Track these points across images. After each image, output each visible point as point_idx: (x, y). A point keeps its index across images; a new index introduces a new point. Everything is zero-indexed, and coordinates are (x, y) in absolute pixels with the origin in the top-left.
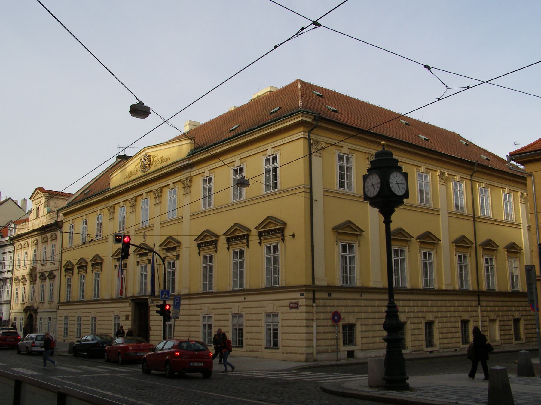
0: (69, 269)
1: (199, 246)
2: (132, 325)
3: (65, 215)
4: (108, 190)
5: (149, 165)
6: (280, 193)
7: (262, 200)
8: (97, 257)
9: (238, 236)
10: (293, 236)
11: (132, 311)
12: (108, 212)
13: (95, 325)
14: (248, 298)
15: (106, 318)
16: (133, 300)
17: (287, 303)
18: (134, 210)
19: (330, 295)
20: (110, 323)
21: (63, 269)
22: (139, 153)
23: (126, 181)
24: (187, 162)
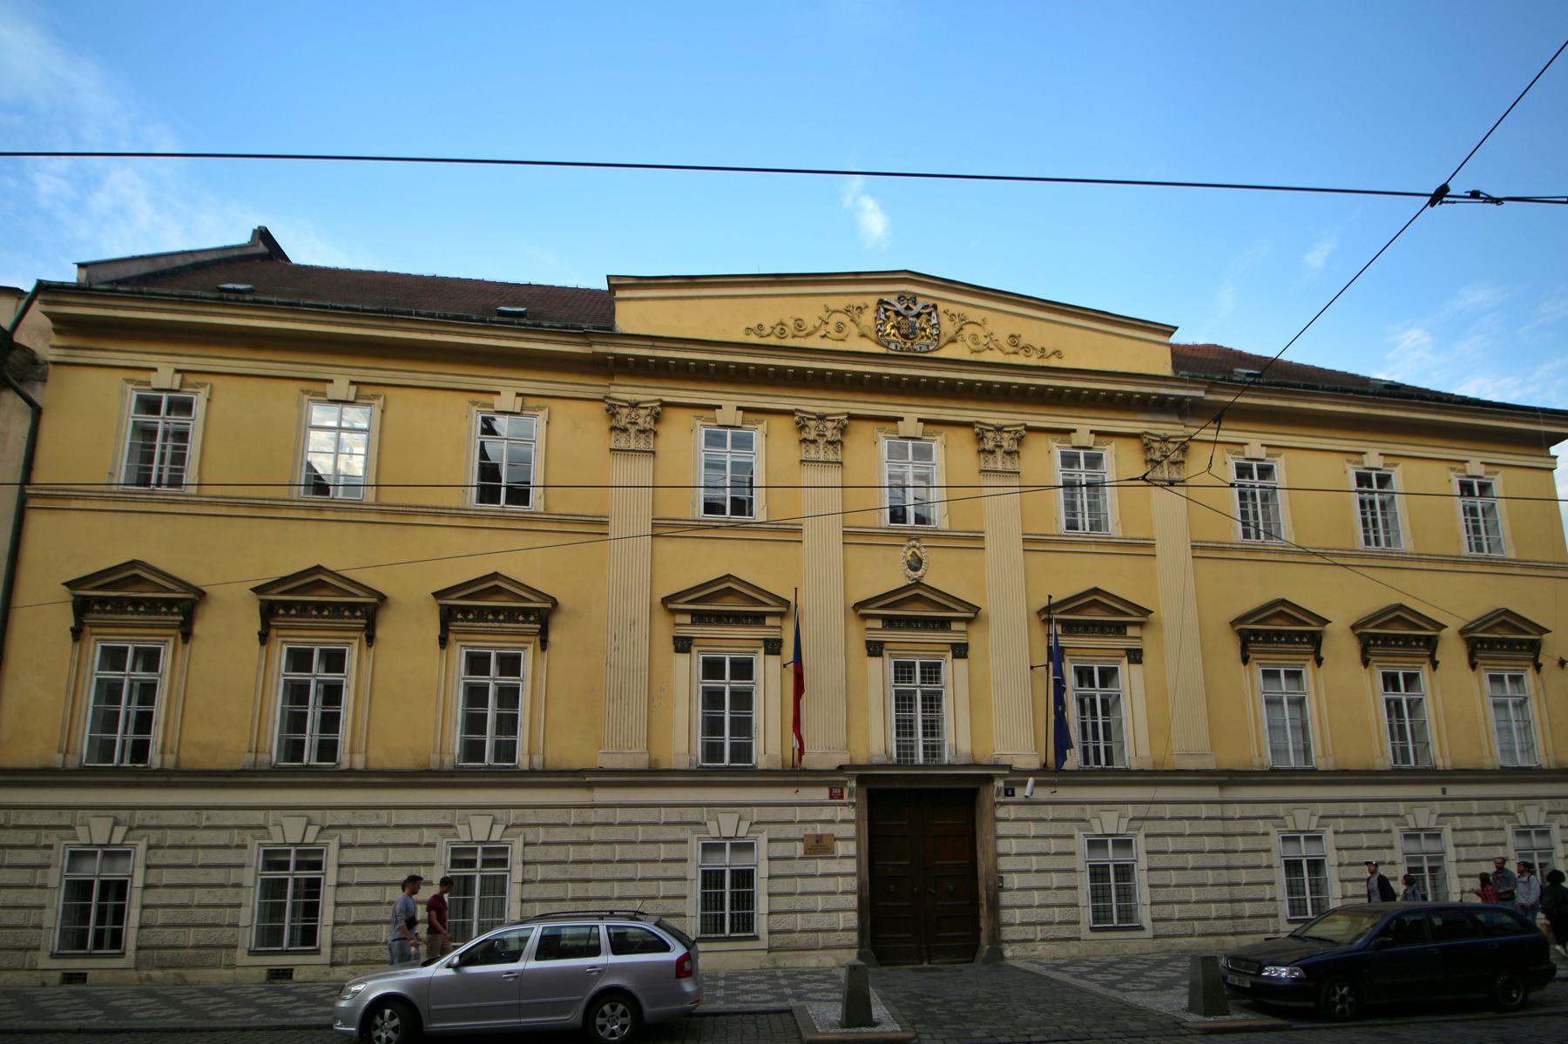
3: (65, 325)
4: (607, 330)
7: (1461, 568)
9: (1396, 638)
14: (1453, 791)
16: (861, 780)
19: (1444, 792)
23: (753, 339)
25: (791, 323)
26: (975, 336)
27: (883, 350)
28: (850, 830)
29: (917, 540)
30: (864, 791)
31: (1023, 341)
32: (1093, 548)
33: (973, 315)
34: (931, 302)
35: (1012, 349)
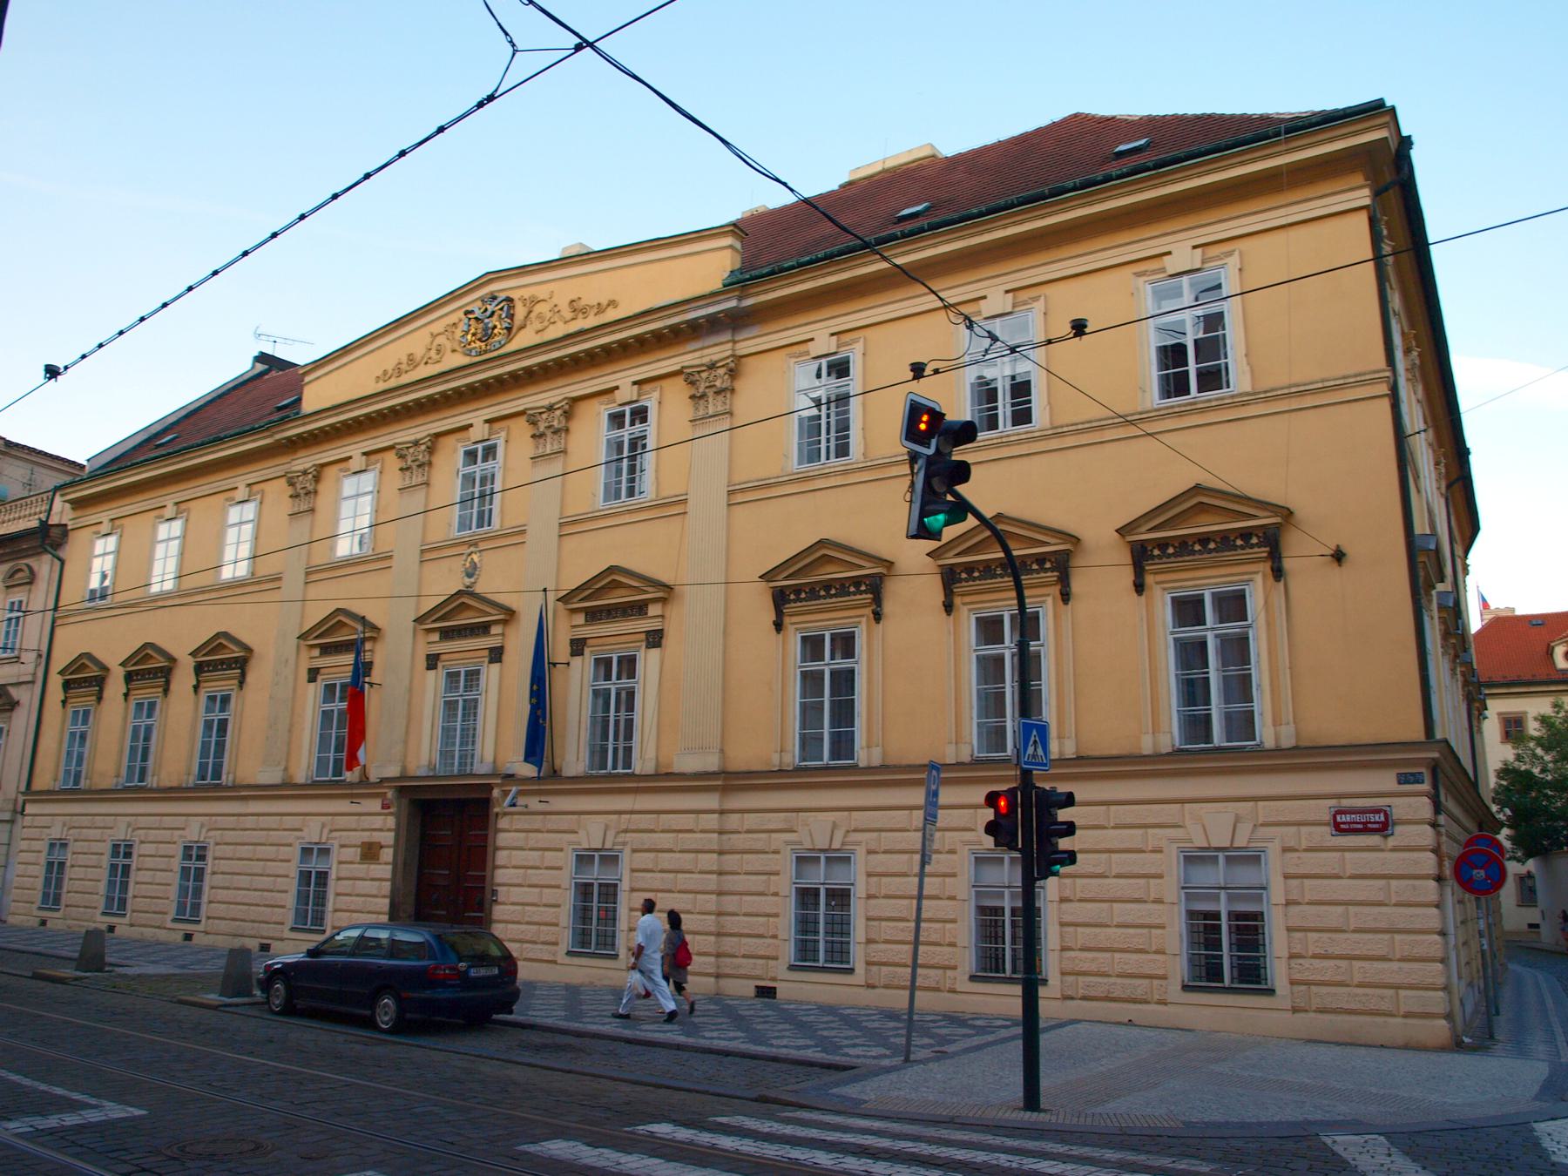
0: (85, 678)
1: (780, 599)
2: (393, 880)
5: (509, 329)
6: (1244, 404)
8: (146, 651)
10: (1339, 556)
11: (397, 830)
12: (290, 491)
13: (126, 869)
15: (244, 851)
16: (402, 791)
17: (1323, 810)
18: (420, 480)
20: (280, 868)
21: (56, 682)
22: (453, 296)
23: (382, 386)
24: (733, 303)
25: (404, 359)
26: (540, 316)
27: (466, 360)
28: (388, 838)
29: (476, 545)
30: (405, 801)
31: (583, 303)
32: (627, 518)
33: (541, 292)
34: (502, 296)
35: (571, 315)
